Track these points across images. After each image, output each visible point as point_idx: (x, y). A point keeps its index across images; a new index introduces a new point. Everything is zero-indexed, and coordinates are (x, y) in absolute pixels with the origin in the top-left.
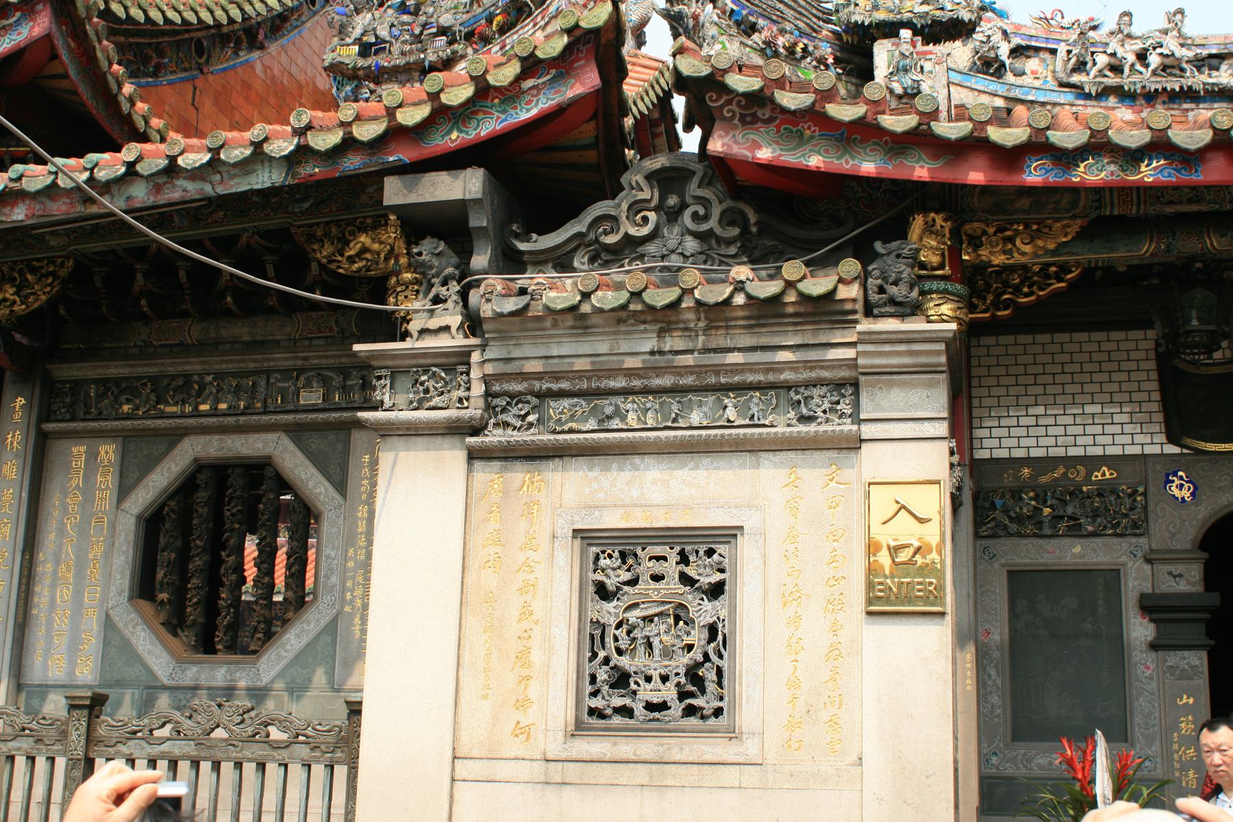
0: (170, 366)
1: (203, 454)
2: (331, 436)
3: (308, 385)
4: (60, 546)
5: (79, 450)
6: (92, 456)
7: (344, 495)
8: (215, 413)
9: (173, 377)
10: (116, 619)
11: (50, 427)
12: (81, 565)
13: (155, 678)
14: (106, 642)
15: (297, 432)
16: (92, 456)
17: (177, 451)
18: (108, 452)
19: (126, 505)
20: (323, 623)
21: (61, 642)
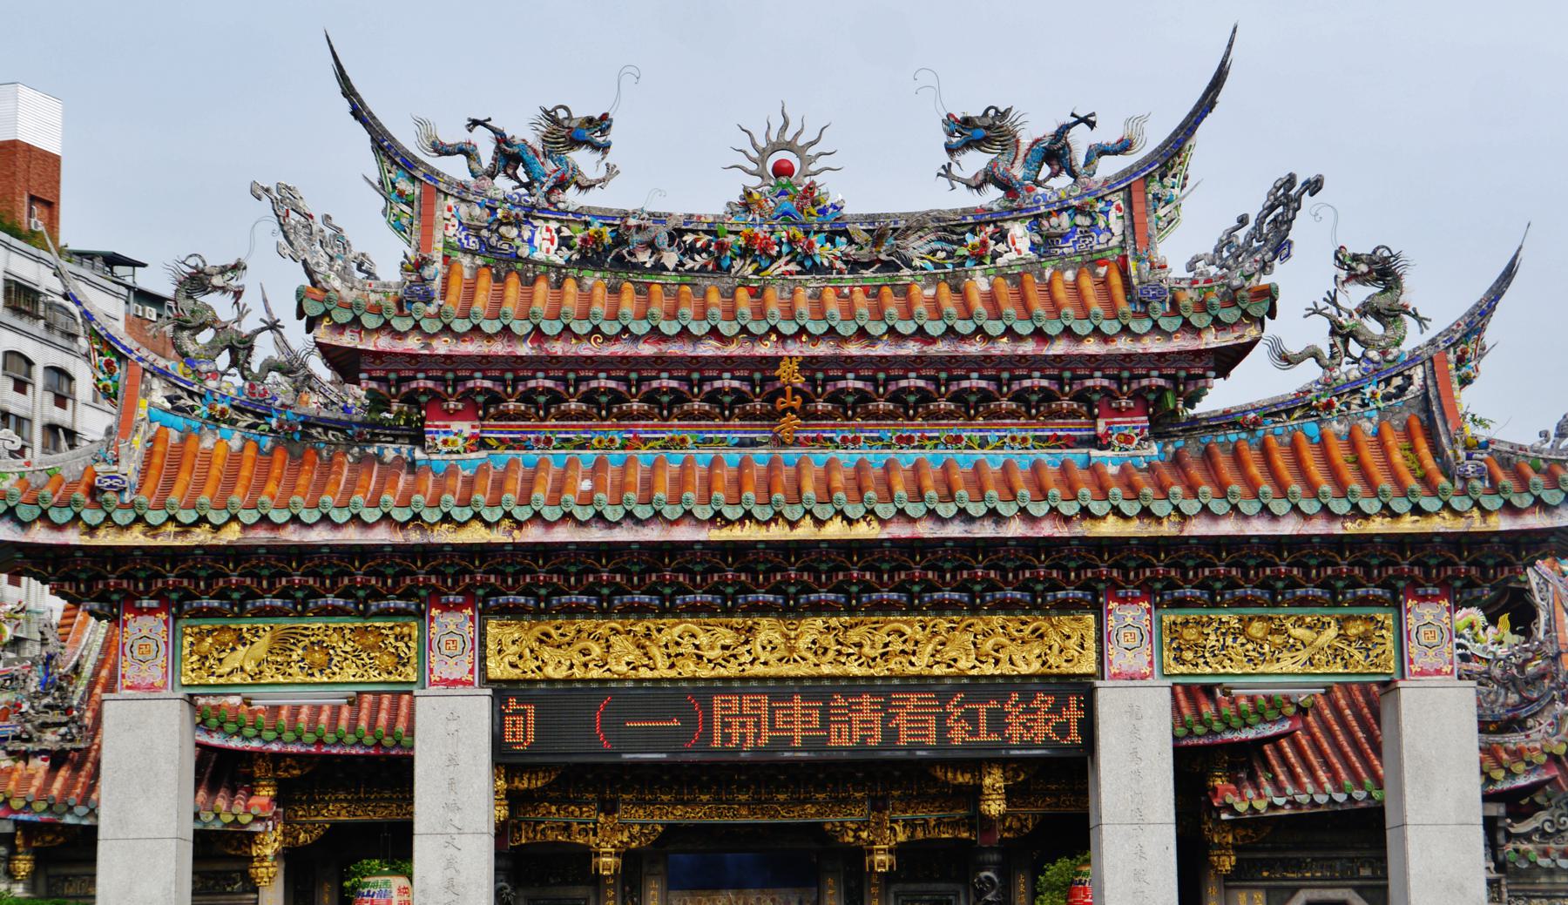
0: (1290, 855)
3: (1363, 866)
6: (1251, 898)
8: (1314, 878)
15: (1359, 890)
16: (1251, 898)
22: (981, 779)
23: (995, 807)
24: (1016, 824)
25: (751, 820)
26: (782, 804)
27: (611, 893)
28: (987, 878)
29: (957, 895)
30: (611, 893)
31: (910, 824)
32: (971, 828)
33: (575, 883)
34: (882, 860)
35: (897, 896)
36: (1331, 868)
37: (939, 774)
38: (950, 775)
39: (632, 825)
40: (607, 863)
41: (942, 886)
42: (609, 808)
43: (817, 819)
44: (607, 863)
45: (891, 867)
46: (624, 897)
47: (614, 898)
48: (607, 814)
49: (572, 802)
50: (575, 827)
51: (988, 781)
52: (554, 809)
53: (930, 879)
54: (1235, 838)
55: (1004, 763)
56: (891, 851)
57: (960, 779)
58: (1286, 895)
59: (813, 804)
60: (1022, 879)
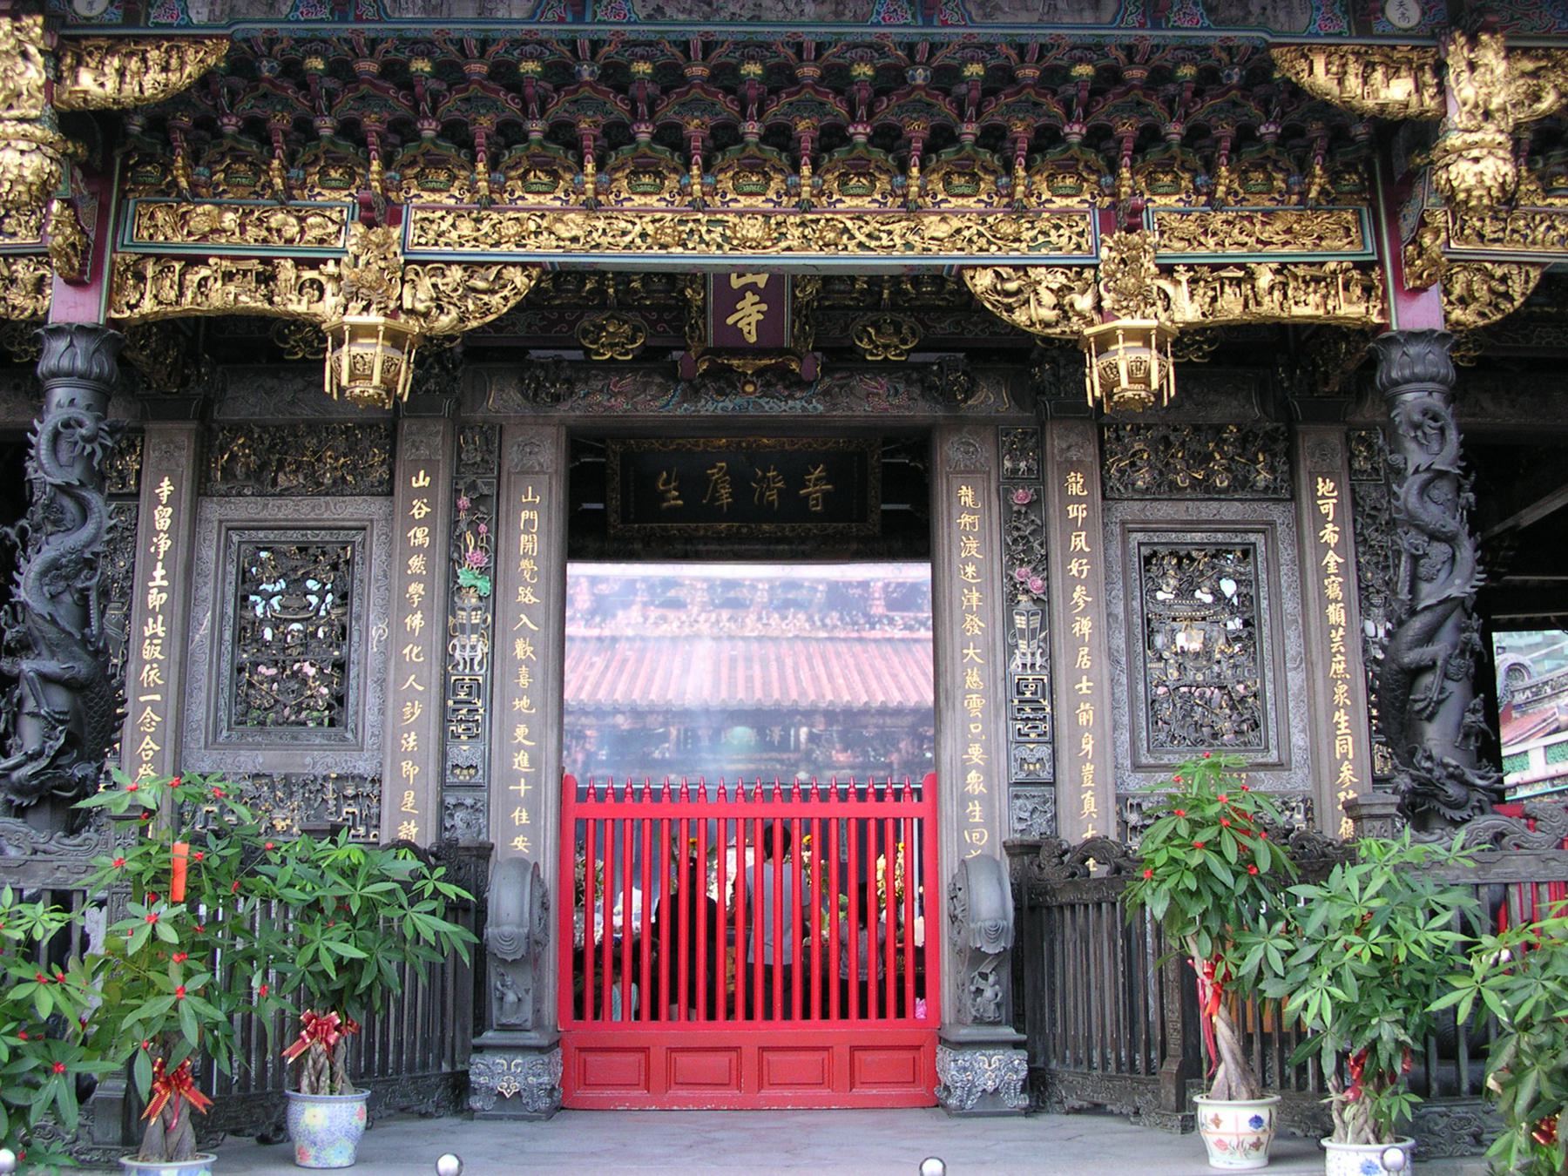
22: (1442, 90)
23: (1477, 165)
24: (1481, 290)
26: (858, 216)
27: (420, 510)
29: (1268, 528)
30: (420, 510)
31: (1207, 275)
33: (339, 488)
35: (1126, 531)
38: (1353, 83)
40: (363, 367)
41: (1231, 511)
43: (950, 257)
44: (363, 367)
48: (370, 224)
49: (284, 201)
50: (287, 272)
51: (1465, 89)
52: (229, 220)
53: (1206, 490)
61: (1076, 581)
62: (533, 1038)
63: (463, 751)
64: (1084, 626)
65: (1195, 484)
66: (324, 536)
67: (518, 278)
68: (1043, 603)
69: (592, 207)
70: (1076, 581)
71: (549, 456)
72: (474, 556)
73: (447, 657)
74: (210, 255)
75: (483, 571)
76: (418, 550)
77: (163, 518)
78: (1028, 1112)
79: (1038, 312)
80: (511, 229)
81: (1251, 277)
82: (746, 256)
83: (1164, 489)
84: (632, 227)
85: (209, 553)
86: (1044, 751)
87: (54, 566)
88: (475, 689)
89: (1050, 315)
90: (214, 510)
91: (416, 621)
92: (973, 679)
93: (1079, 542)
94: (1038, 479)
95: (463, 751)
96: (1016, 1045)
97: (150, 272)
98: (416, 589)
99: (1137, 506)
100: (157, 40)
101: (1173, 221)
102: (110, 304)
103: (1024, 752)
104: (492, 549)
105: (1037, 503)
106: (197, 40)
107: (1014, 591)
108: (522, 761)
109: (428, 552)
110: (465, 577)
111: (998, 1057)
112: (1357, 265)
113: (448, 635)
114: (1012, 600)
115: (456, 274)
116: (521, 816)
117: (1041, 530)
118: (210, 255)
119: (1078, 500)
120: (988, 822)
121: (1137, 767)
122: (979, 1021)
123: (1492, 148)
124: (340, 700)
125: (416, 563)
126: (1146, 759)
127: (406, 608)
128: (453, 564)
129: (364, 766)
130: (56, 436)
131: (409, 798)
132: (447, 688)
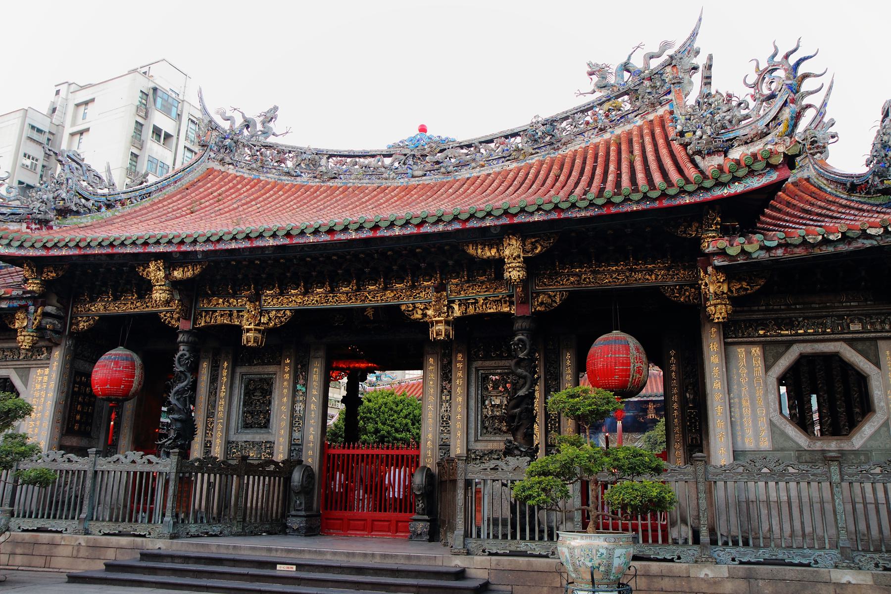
1: (804, 351)
2: (868, 343)
3: (852, 322)
4: (740, 391)
5: (741, 351)
7: (880, 368)
9: (783, 319)
10: (775, 422)
11: (730, 340)
12: (753, 401)
13: (801, 447)
14: (773, 432)
15: (851, 342)
16: (748, 353)
17: (791, 349)
18: (756, 351)
19: (770, 373)
20: (881, 422)
21: (749, 432)
23: (514, 273)
25: (349, 304)
27: (287, 369)
28: (520, 340)
31: (464, 303)
32: (511, 303)
33: (269, 363)
34: (439, 330)
35: (477, 370)
36: (825, 326)
37: (471, 250)
38: (479, 251)
39: (268, 312)
40: (249, 338)
42: (255, 298)
43: (395, 302)
45: (447, 335)
46: (296, 372)
47: (289, 372)
49: (234, 296)
50: (235, 314)
51: (507, 252)
54: (729, 290)
55: (522, 231)
56: (447, 323)
57: (488, 254)
58: (781, 349)
59: (392, 291)
60: (568, 356)
61: (458, 386)
62: (303, 513)
63: (296, 435)
64: (460, 399)
65: (497, 355)
66: (266, 376)
67: (288, 313)
68: (450, 392)
69: (305, 294)
70: (458, 386)
71: (321, 353)
72: (301, 381)
73: (293, 410)
74: (219, 311)
75: (304, 385)
76: (286, 380)
77: (225, 373)
78: (430, 540)
79: (418, 315)
80: (285, 301)
81: (477, 302)
82: (342, 305)
83: (487, 357)
84: (317, 299)
85: (237, 382)
86: (448, 436)
87: (177, 391)
88: (300, 418)
89: (420, 316)
90: (240, 370)
91: (285, 399)
92: (430, 415)
93: (460, 374)
94: (450, 356)
95: (296, 435)
96: (427, 521)
97: (204, 314)
98: (285, 391)
99: (480, 362)
100: (191, 263)
101: (453, 287)
102: (195, 323)
103: (442, 436)
104: (306, 380)
105: (450, 363)
106: (200, 263)
107: (443, 389)
108: (311, 437)
109: (288, 381)
110: (299, 387)
111: (421, 524)
112: (508, 296)
113: (294, 402)
114: (442, 392)
115: (274, 312)
116: (310, 453)
117: (450, 371)
118: (219, 311)
119: (460, 362)
120: (432, 456)
121: (477, 441)
122: (418, 514)
123: (514, 268)
124: (268, 421)
125: (285, 383)
126: (480, 438)
127: (282, 396)
128: (295, 383)
129: (271, 439)
130: (179, 358)
131: (281, 447)
132: (292, 417)
